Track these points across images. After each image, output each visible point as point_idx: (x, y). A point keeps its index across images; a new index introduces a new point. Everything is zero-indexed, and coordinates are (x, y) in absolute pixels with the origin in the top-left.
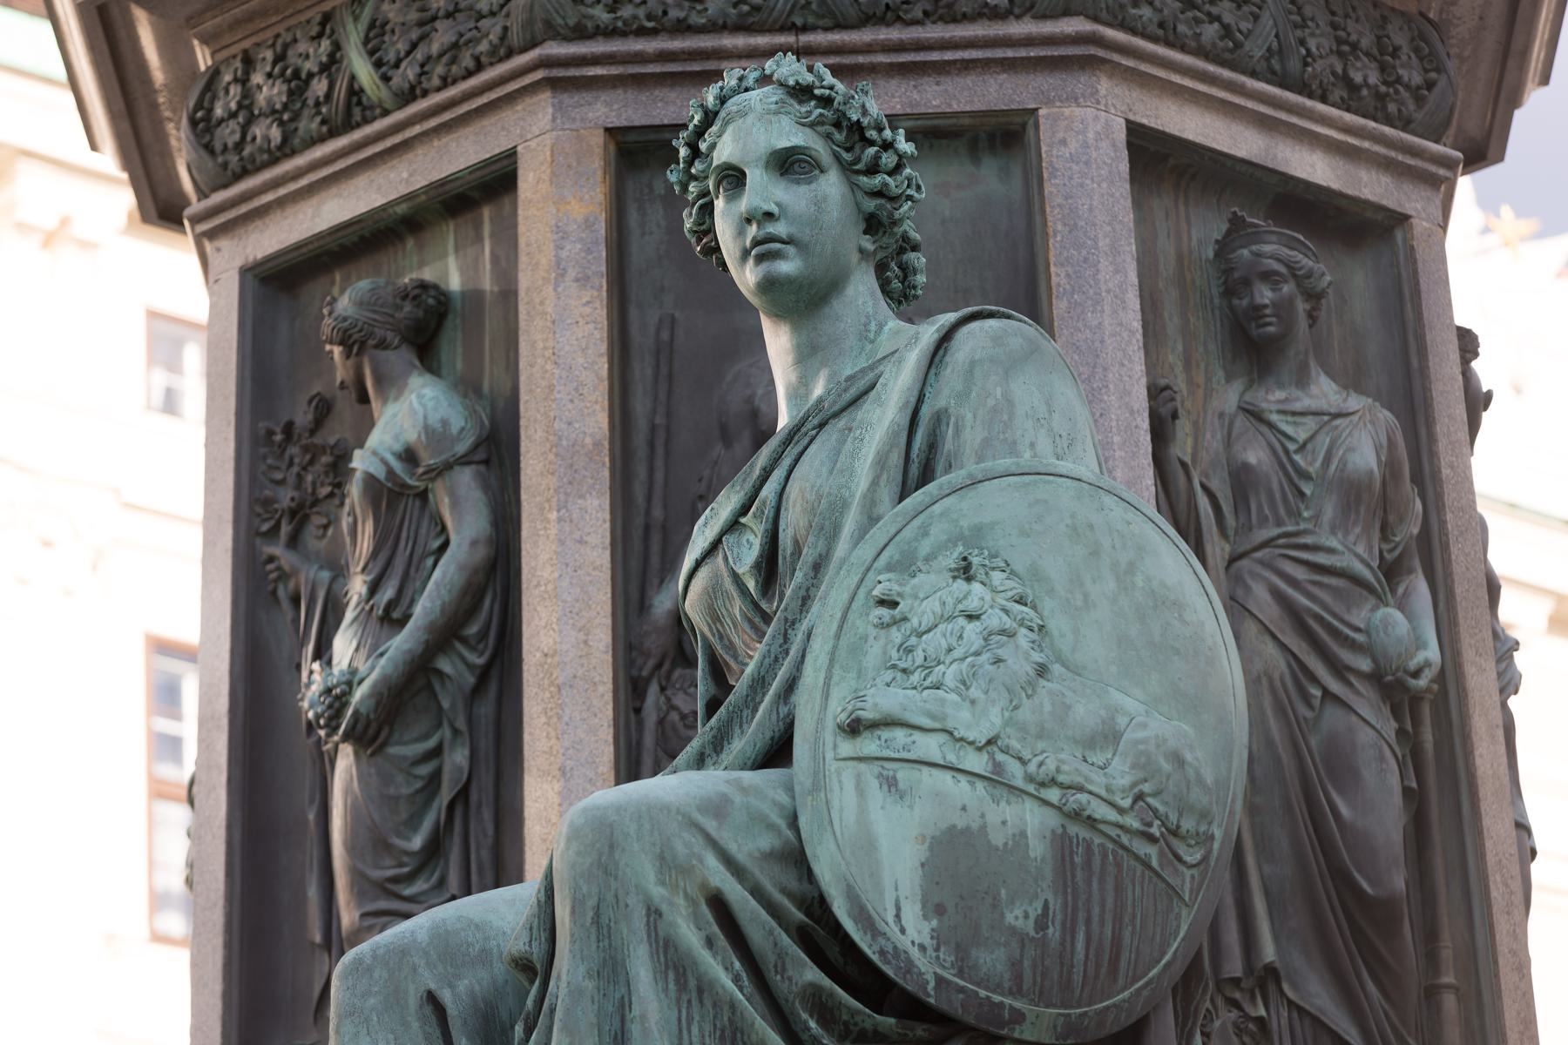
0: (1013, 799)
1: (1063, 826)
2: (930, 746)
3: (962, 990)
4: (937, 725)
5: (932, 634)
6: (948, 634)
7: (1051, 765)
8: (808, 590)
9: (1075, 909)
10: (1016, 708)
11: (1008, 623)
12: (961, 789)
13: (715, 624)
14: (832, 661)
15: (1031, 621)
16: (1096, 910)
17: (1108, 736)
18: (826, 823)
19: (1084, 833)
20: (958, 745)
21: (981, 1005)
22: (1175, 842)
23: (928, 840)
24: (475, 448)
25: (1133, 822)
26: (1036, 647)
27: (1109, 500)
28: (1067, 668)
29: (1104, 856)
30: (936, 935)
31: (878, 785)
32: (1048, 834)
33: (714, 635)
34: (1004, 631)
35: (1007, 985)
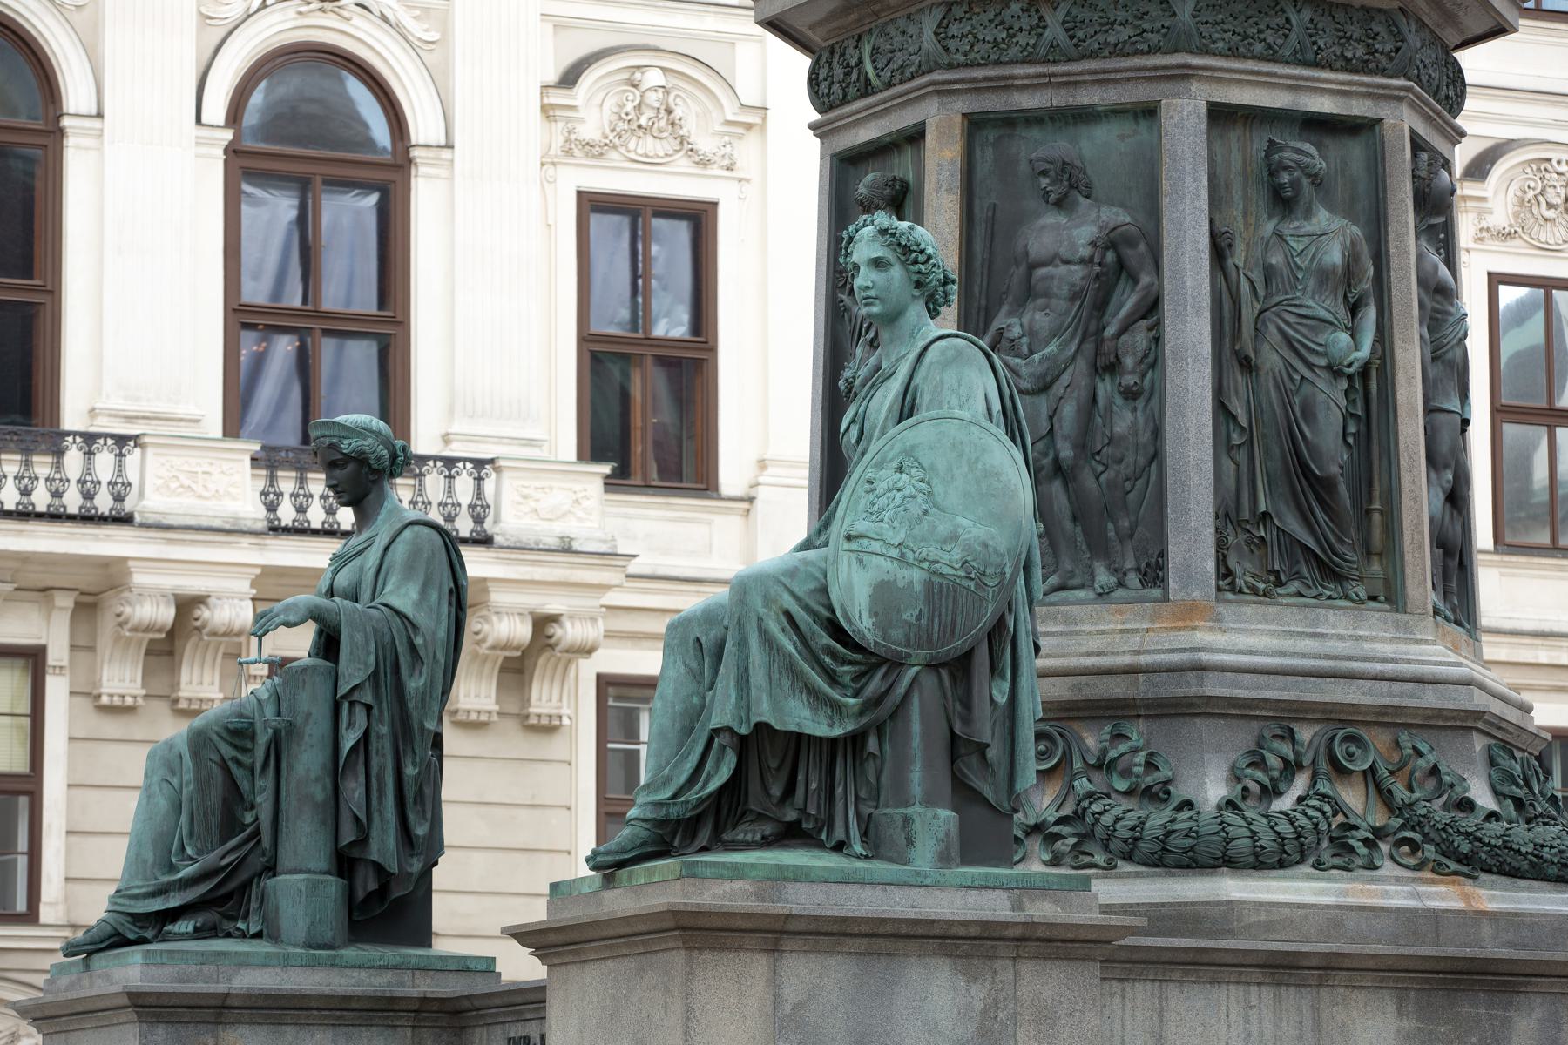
2: (876, 546)
3: (884, 646)
7: (924, 554)
9: (934, 611)
12: (887, 565)
17: (954, 537)
19: (939, 580)
22: (982, 577)
25: (961, 573)
27: (973, 428)
28: (938, 509)
29: (949, 587)
30: (874, 624)
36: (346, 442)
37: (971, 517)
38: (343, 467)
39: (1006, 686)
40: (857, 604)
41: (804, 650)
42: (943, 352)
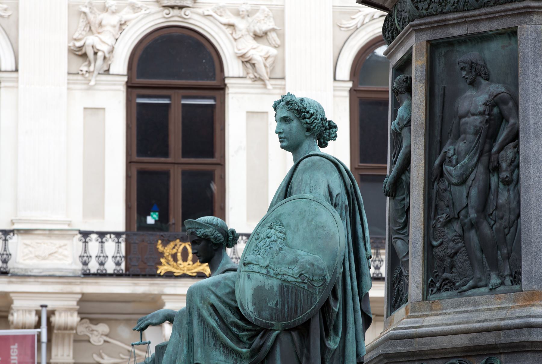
0: (271, 278)
1: (282, 283)
2: (256, 268)
3: (260, 321)
4: (257, 264)
7: (278, 271)
9: (284, 301)
10: (273, 258)
11: (276, 238)
16: (290, 301)
19: (287, 284)
25: (299, 280)
27: (313, 203)
28: (289, 247)
29: (292, 288)
30: (254, 309)
36: (199, 230)
37: (306, 250)
38: (199, 243)
39: (338, 339)
41: (222, 325)
42: (305, 164)
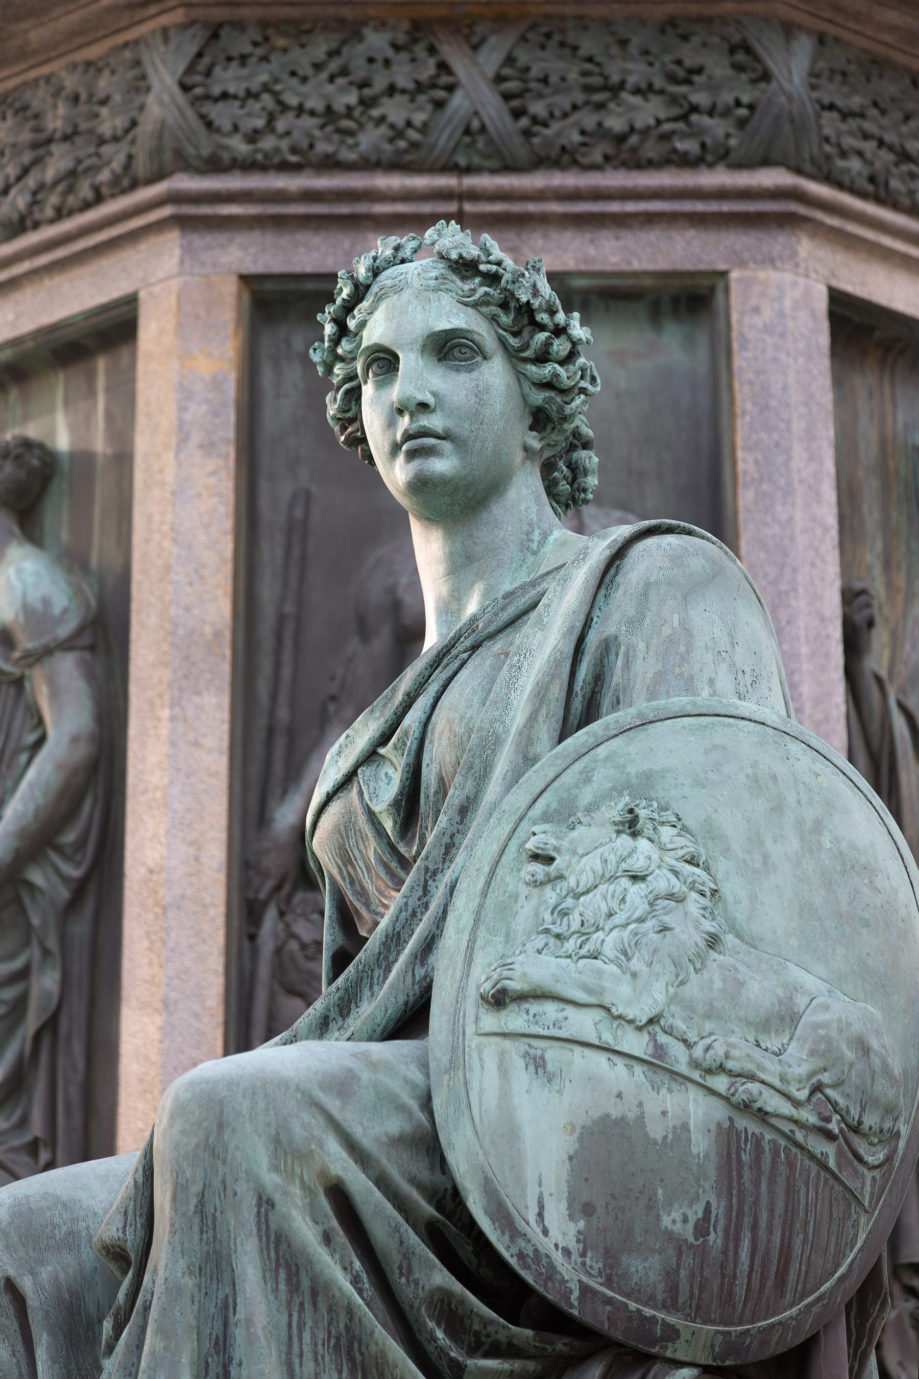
0: (675, 1086)
1: (730, 1119)
3: (609, 1301)
4: (593, 1000)
5: (591, 895)
6: (609, 897)
7: (719, 1050)
8: (452, 836)
9: (740, 1214)
10: (682, 983)
11: (677, 886)
13: (346, 866)
14: (477, 921)
15: (703, 884)
16: (764, 1216)
18: (464, 1106)
19: (754, 1128)
20: (615, 1024)
21: (630, 1319)
22: (856, 1140)
23: (578, 1130)
24: (80, 631)
25: (809, 1116)
26: (707, 915)
27: (795, 748)
28: (741, 939)
29: (776, 1153)
30: (582, 1238)
31: (524, 1066)
32: (713, 1128)
33: (343, 878)
34: (672, 895)
35: (660, 1297)
40: (531, 1177)
